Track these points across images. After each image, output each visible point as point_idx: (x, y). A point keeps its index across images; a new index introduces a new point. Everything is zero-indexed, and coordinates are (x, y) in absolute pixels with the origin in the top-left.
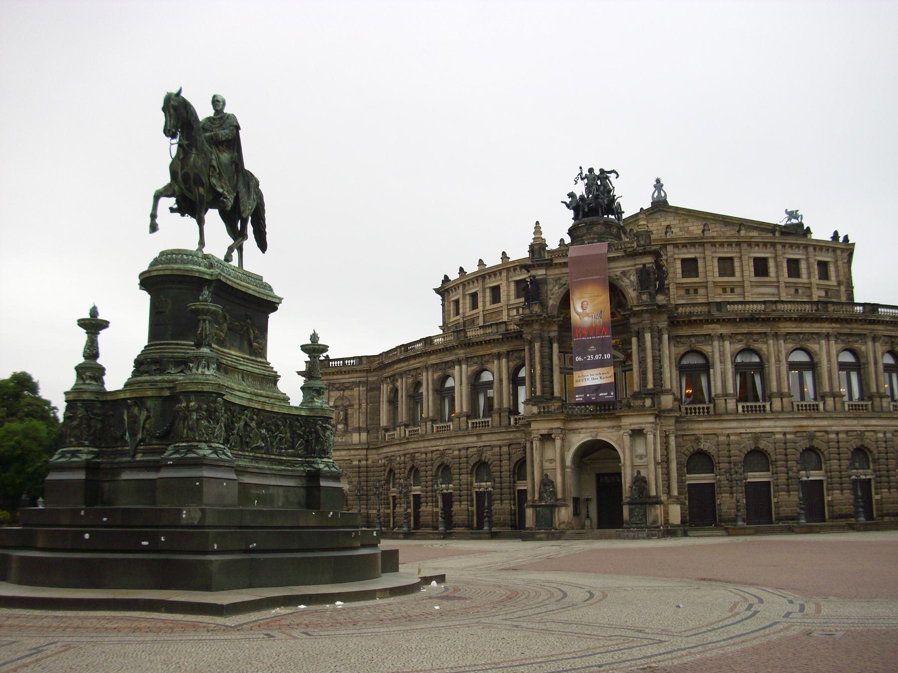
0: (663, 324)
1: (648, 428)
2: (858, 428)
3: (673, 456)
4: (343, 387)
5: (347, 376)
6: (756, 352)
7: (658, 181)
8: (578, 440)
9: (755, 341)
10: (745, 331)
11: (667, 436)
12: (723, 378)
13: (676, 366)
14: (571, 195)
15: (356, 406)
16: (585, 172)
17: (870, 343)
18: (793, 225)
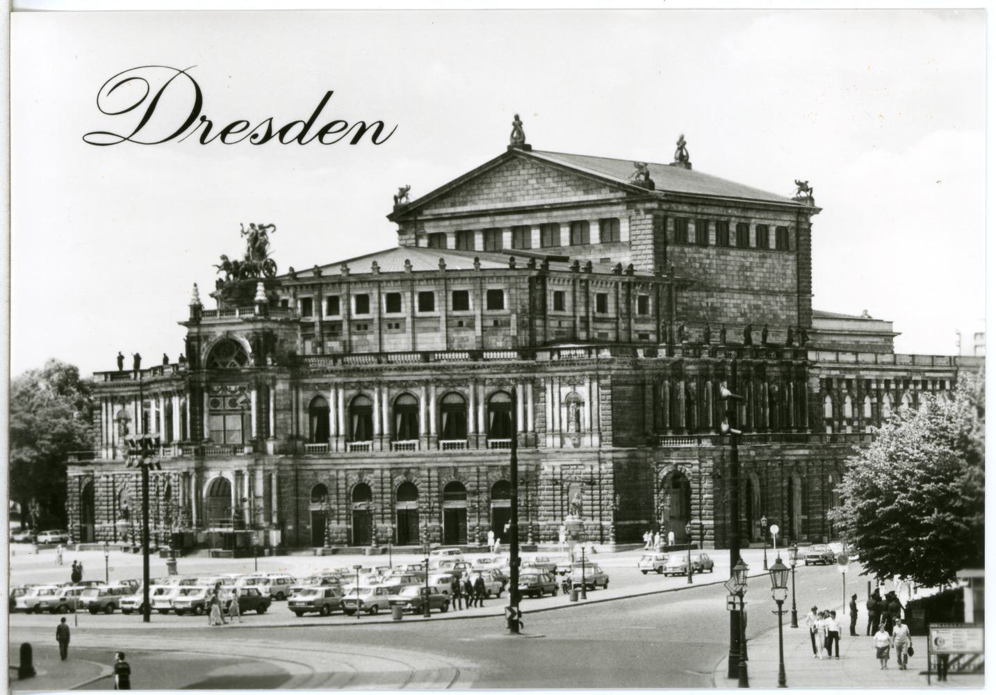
0: (269, 382)
1: (245, 470)
2: (450, 464)
3: (274, 490)
4: (124, 401)
5: (126, 389)
6: (369, 398)
7: (517, 118)
8: (212, 476)
9: (366, 388)
10: (355, 380)
11: (271, 476)
12: (337, 420)
13: (304, 409)
14: (224, 257)
15: (134, 421)
16: (247, 227)
17: (472, 387)
18: (643, 185)
